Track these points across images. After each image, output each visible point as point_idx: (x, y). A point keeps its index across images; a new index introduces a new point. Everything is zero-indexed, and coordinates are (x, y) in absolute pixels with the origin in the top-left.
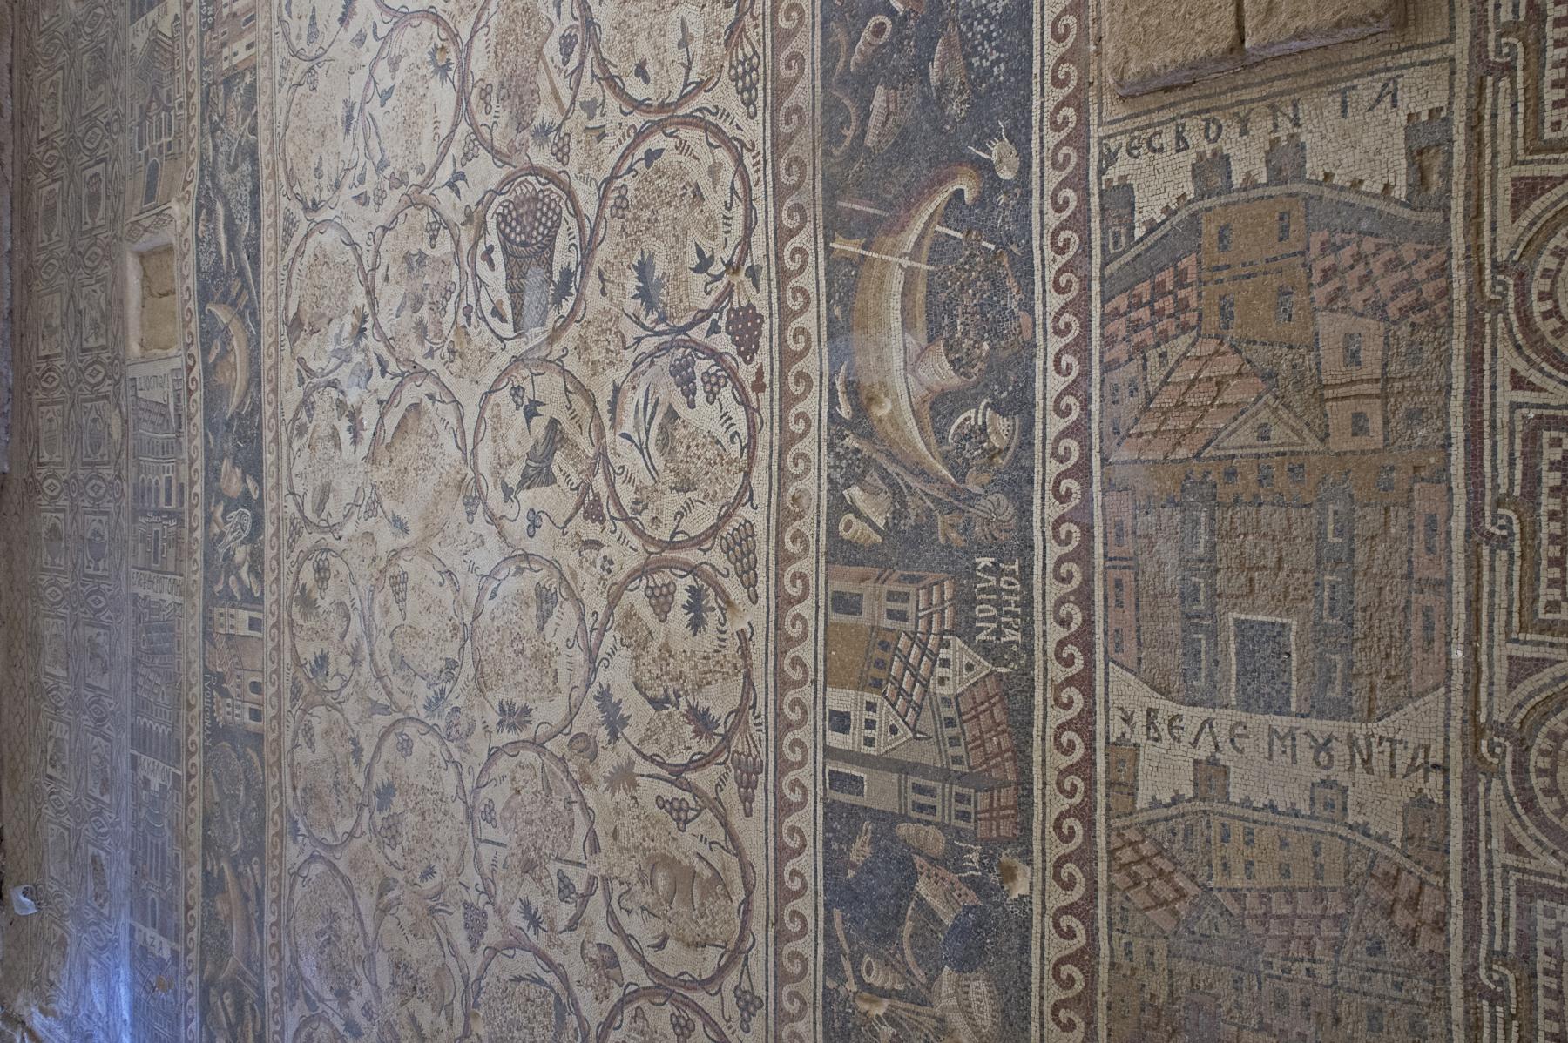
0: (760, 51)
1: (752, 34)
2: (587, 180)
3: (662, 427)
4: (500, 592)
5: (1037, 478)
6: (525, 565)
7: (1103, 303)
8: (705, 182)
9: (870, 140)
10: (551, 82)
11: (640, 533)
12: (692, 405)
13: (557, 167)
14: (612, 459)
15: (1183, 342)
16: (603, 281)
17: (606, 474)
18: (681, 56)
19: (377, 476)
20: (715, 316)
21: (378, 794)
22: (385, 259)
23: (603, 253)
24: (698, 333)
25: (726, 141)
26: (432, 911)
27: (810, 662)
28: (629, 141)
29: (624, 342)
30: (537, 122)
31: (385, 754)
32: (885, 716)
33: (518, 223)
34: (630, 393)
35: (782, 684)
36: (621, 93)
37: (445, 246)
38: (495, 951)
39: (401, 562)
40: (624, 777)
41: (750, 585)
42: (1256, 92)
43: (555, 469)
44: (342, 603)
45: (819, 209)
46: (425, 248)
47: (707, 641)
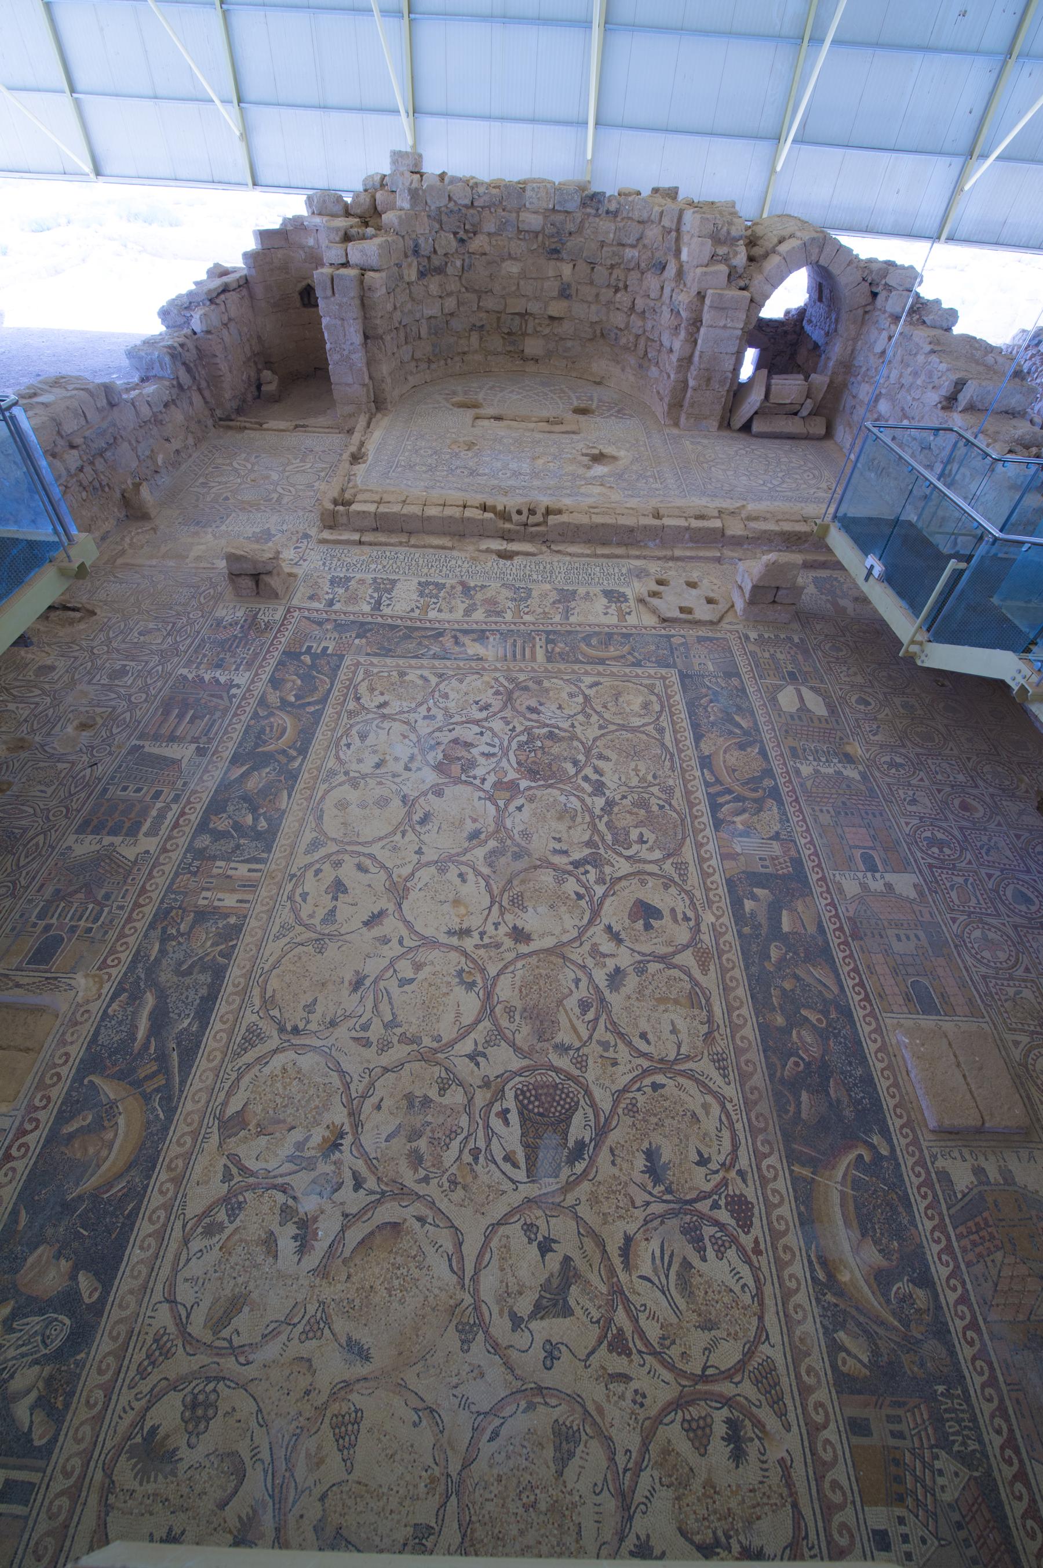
2: (603, 1086)
3: (678, 1274)
4: (503, 1432)
5: (952, 1329)
6: (540, 1400)
7: (955, 1228)
8: (700, 1112)
9: (804, 1116)
10: (570, 1021)
11: (671, 1367)
12: (704, 1259)
13: (577, 1073)
14: (632, 1298)
15: (999, 1255)
16: (613, 1155)
17: (628, 1311)
18: (673, 1037)
19: (327, 1292)
20: (716, 1197)
22: (380, 1092)
23: (614, 1137)
24: (704, 1206)
25: (711, 1092)
27: (845, 1483)
29: (633, 1202)
32: (914, 1528)
33: (536, 1099)
34: (644, 1243)
35: (828, 1510)
36: (629, 1044)
37: (456, 1097)
39: (354, 1397)
41: (782, 1414)
42: (984, 1144)
43: (572, 1302)
44: (234, 1454)
45: (781, 1146)
46: (433, 1093)
47: (750, 1473)
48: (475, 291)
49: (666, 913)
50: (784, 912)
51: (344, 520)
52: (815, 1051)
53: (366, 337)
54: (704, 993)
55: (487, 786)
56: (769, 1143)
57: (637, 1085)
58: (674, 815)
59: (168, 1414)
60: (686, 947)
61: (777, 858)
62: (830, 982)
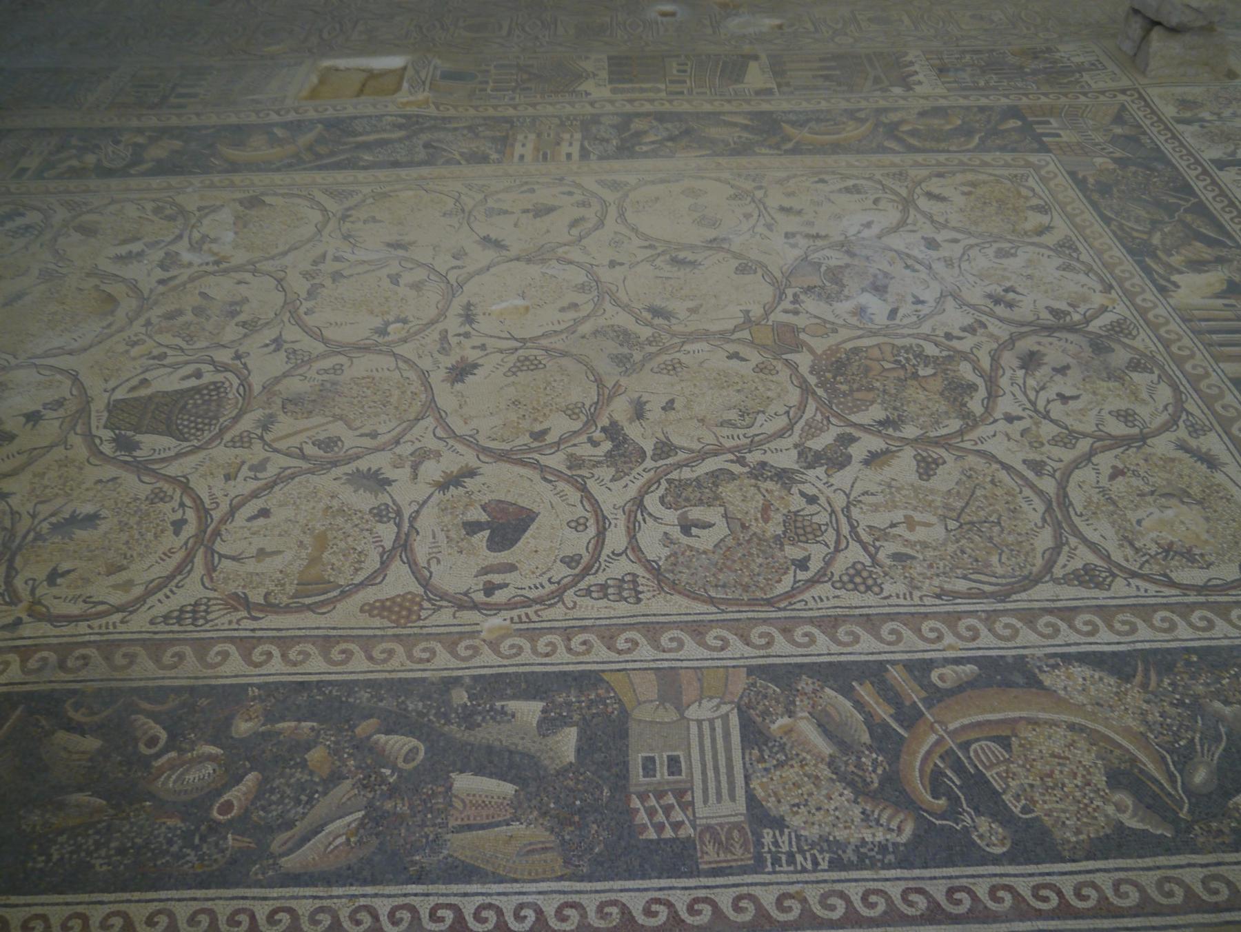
0: (207, 627)
1: (225, 620)
9: (61, 736)
10: (308, 429)
18: (253, 550)
25: (149, 593)
28: (207, 501)
30: (282, 417)
36: (255, 495)
49: (504, 557)
50: (509, 789)
52: (168, 784)
54: (323, 603)
55: (778, 316)
56: (40, 670)
57: (188, 502)
58: (781, 588)
60: (425, 583)
61: (687, 806)
62: (308, 856)
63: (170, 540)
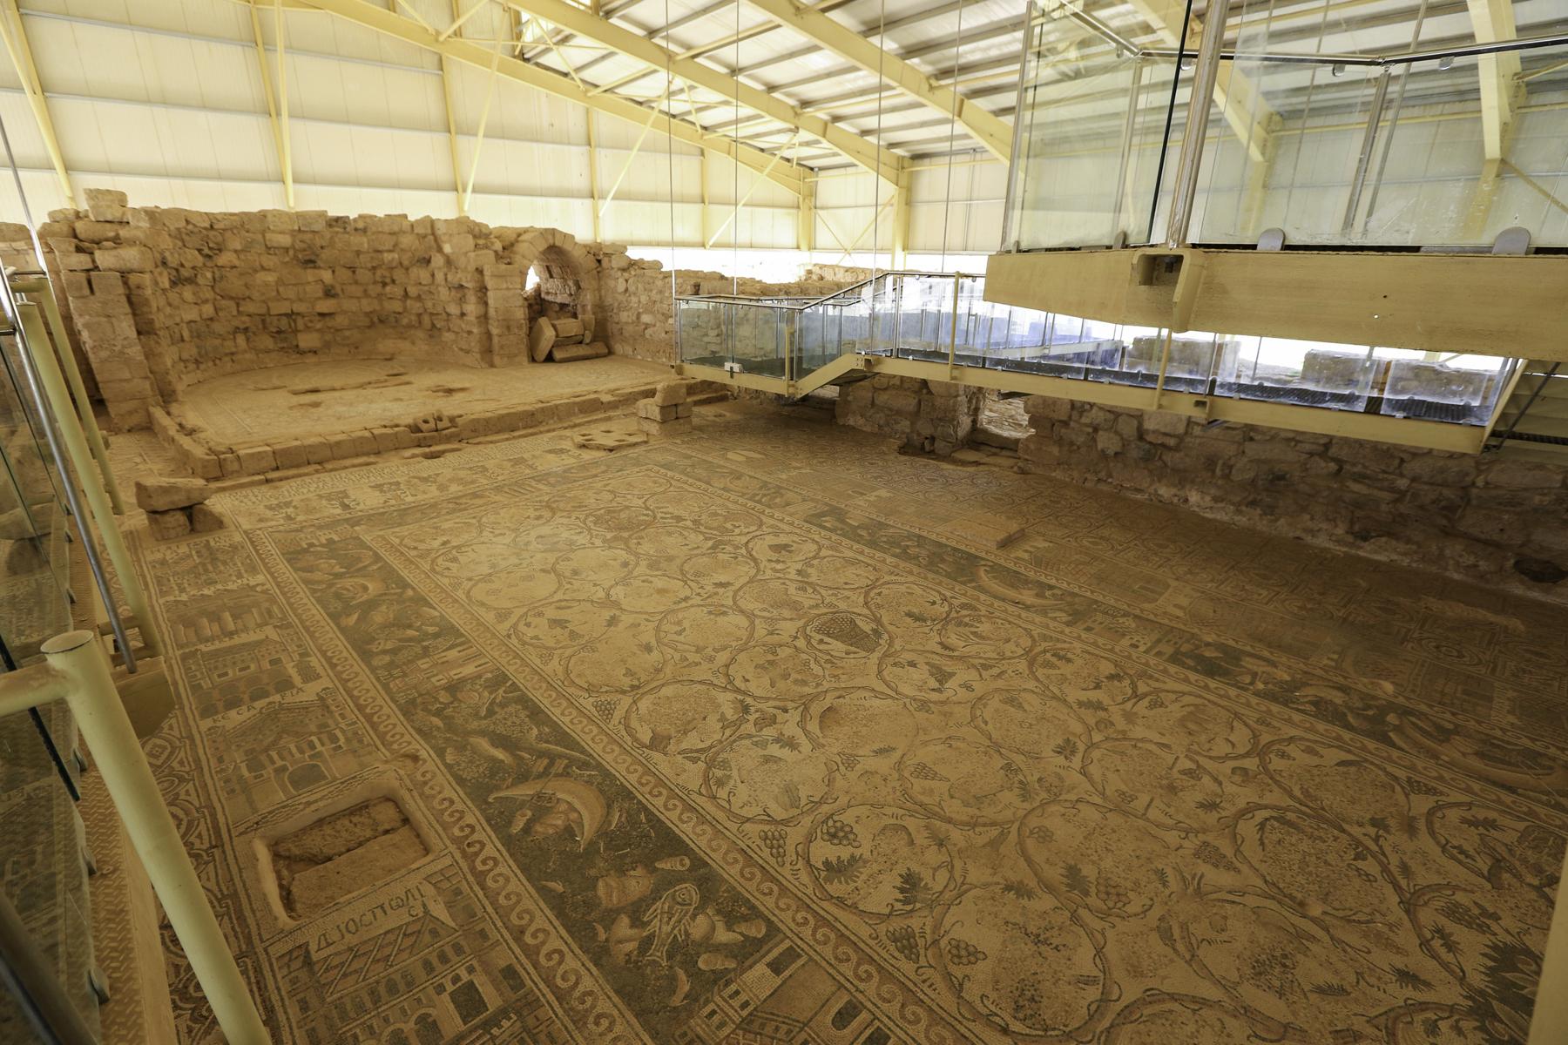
21: (1071, 887)
26: (1198, 890)
31: (1039, 857)
35: (1112, 650)
38: (1238, 851)
40: (1130, 717)
47: (1079, 662)
48: (232, 298)
51: (236, 466)
53: (139, 333)
59: (823, 851)
63: (885, 592)
